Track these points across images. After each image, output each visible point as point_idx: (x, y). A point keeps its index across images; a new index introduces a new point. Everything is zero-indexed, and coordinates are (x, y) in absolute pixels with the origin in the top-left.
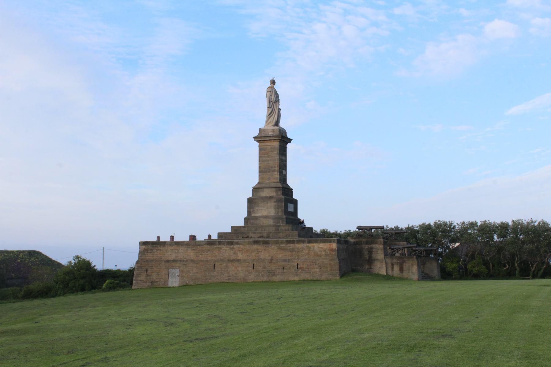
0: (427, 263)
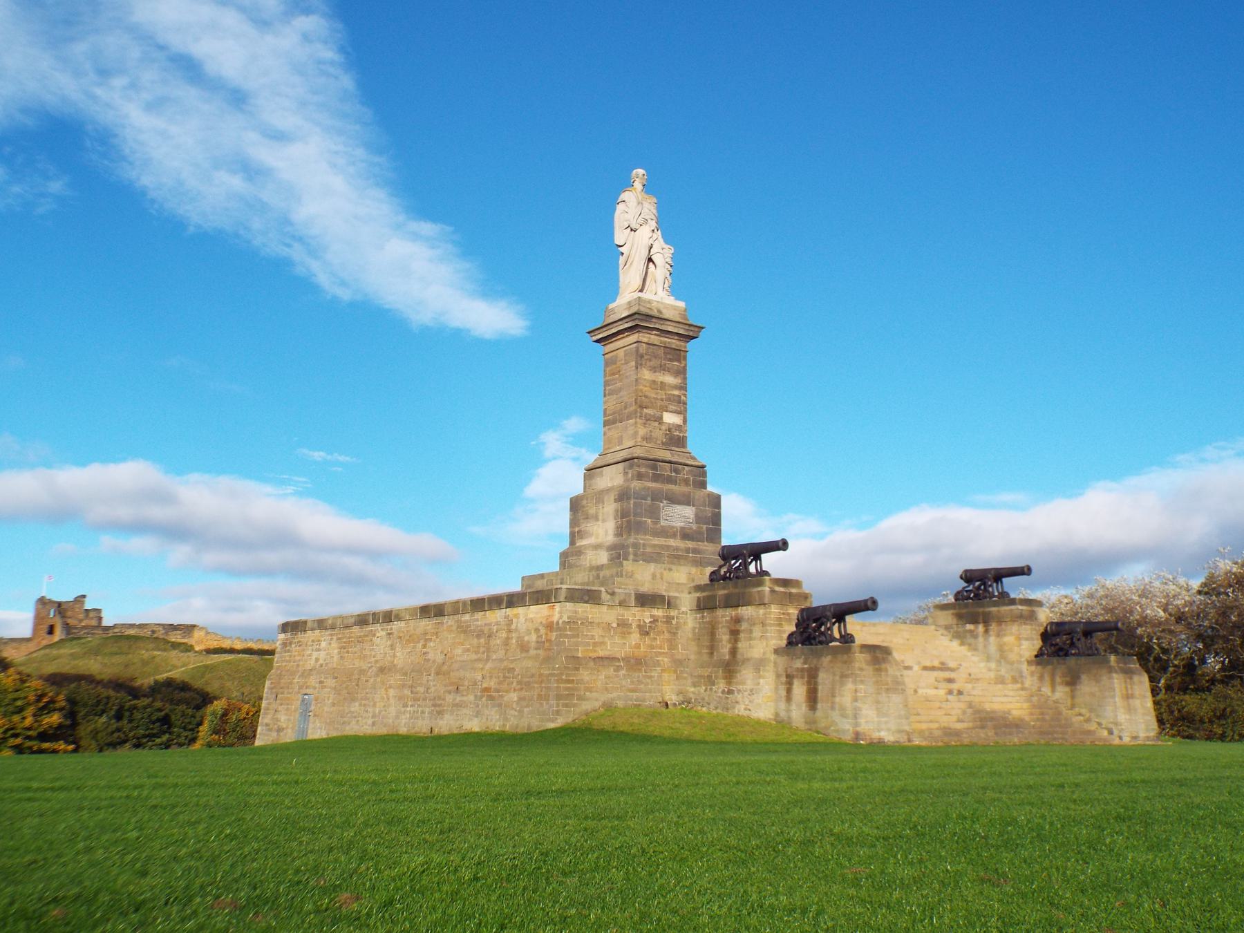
0: (1084, 677)
